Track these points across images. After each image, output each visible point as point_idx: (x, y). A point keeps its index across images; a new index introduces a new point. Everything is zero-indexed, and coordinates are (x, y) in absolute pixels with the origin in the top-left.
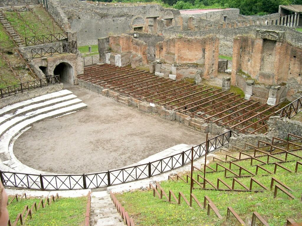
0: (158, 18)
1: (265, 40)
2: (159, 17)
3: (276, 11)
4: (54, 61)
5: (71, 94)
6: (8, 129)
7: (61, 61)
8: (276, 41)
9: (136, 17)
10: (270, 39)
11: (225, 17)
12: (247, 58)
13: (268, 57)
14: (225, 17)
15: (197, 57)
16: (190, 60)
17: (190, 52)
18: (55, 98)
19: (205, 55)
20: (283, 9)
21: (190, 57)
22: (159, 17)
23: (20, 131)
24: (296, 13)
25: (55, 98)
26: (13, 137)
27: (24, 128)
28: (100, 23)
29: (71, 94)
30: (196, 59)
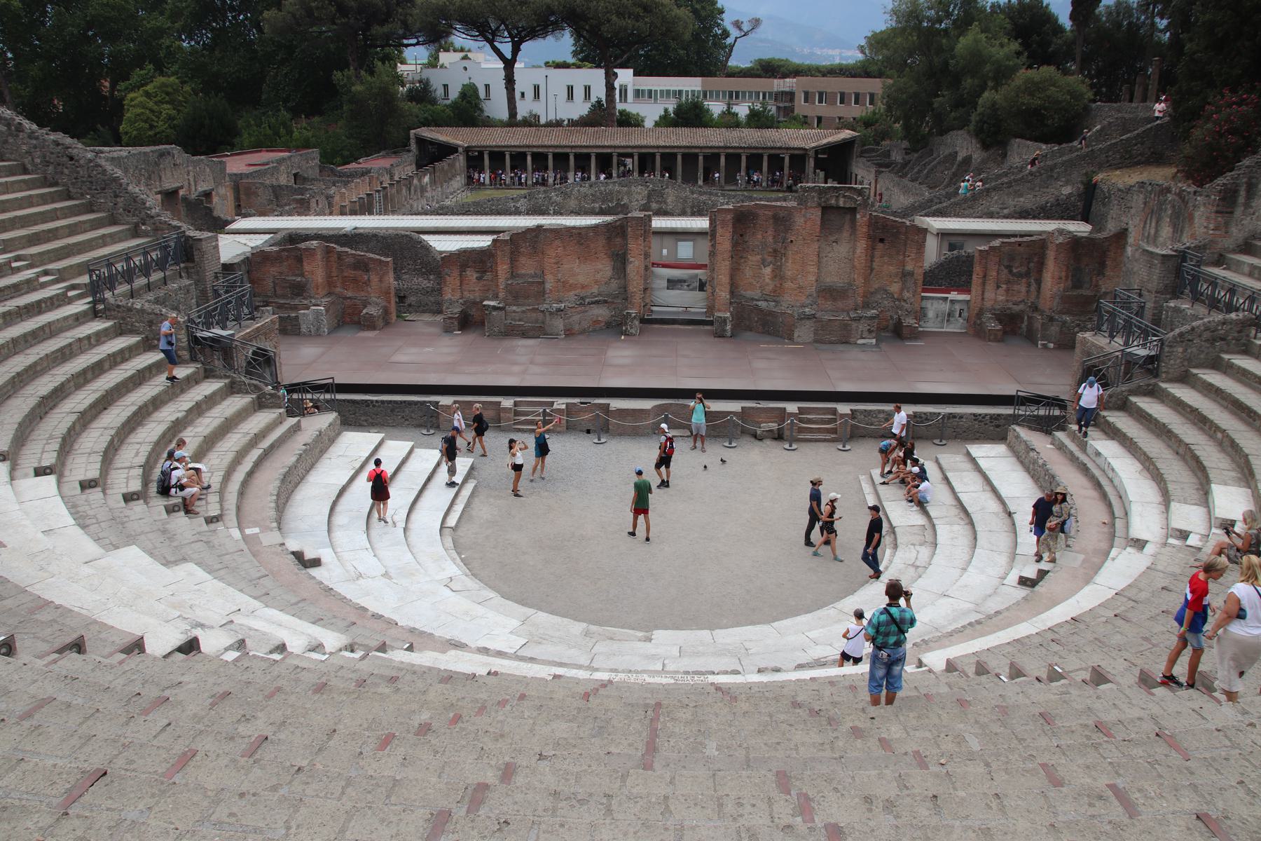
0: (181, 193)
1: (826, 209)
2: (182, 187)
3: (403, 145)
8: (855, 209)
10: (841, 204)
11: (295, 175)
12: (754, 259)
13: (829, 249)
14: (295, 175)
15: (598, 276)
16: (583, 287)
20: (421, 141)
21: (581, 279)
22: (182, 187)
24: (460, 150)
30: (596, 282)
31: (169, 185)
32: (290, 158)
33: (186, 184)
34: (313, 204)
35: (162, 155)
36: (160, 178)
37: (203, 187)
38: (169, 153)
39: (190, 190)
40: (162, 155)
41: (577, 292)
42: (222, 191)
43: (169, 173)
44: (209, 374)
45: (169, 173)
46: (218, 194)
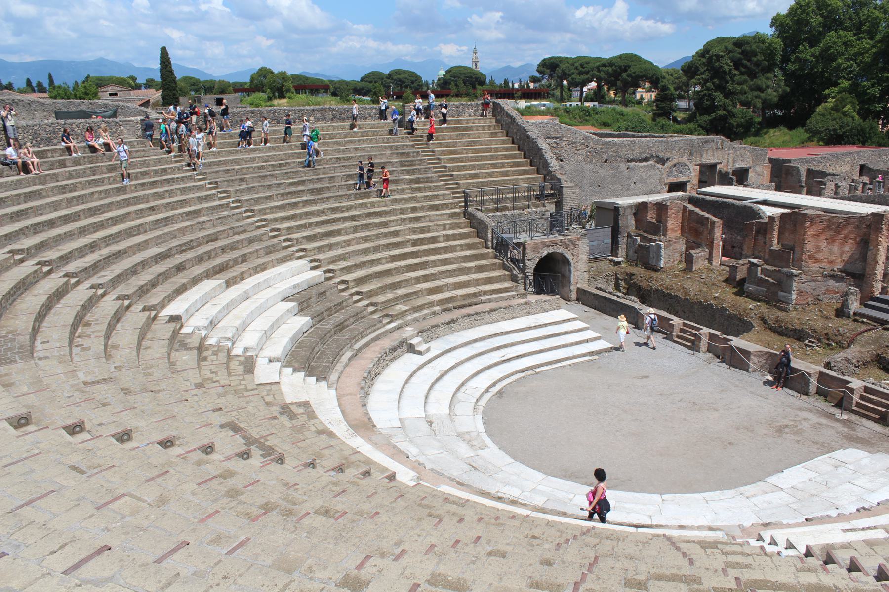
0: (718, 167)
2: (720, 163)
4: (539, 246)
5: (575, 319)
6: (463, 384)
7: (551, 250)
9: (675, 161)
14: (862, 167)
16: (829, 262)
17: (830, 246)
18: (546, 325)
19: (869, 253)
21: (828, 256)
22: (720, 163)
23: (487, 390)
25: (546, 325)
26: (477, 400)
27: (494, 385)
28: (602, 172)
29: (575, 319)
31: (708, 159)
32: (858, 153)
33: (725, 161)
34: (830, 186)
35: (706, 142)
36: (702, 156)
37: (740, 165)
38: (713, 141)
39: (727, 165)
40: (706, 142)
41: (822, 265)
42: (758, 169)
43: (710, 154)
44: (496, 257)
45: (710, 154)
46: (755, 171)
